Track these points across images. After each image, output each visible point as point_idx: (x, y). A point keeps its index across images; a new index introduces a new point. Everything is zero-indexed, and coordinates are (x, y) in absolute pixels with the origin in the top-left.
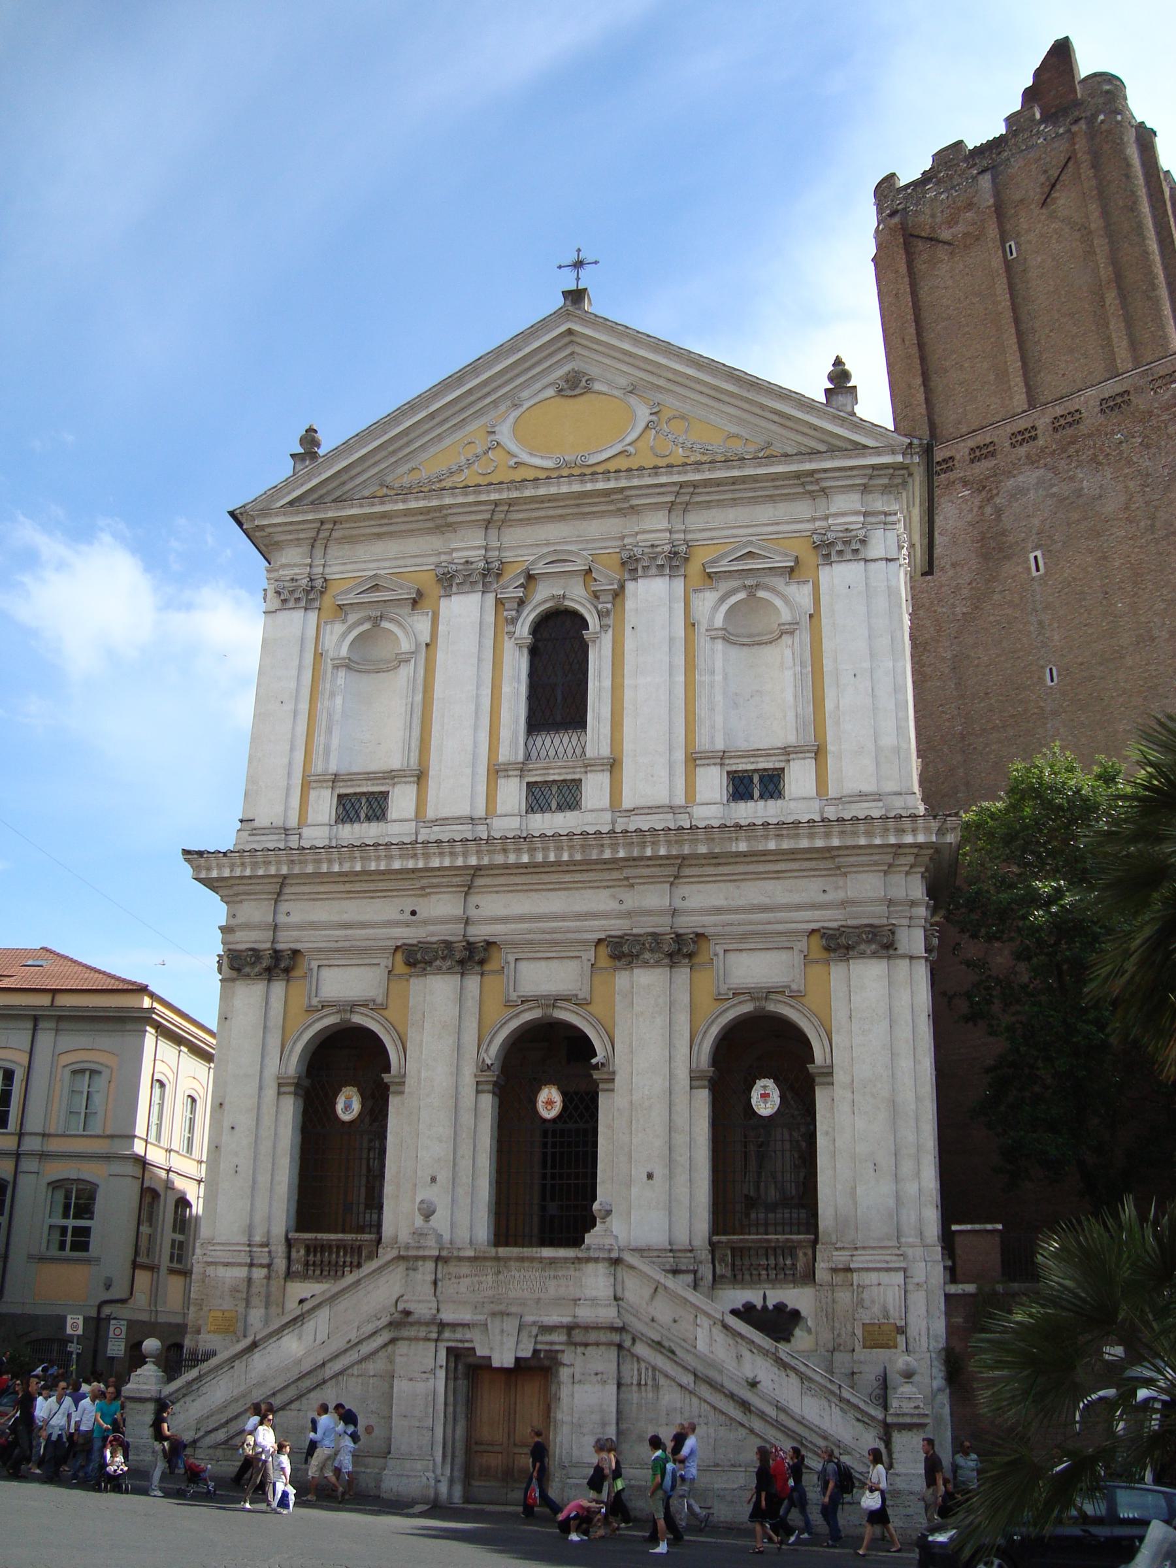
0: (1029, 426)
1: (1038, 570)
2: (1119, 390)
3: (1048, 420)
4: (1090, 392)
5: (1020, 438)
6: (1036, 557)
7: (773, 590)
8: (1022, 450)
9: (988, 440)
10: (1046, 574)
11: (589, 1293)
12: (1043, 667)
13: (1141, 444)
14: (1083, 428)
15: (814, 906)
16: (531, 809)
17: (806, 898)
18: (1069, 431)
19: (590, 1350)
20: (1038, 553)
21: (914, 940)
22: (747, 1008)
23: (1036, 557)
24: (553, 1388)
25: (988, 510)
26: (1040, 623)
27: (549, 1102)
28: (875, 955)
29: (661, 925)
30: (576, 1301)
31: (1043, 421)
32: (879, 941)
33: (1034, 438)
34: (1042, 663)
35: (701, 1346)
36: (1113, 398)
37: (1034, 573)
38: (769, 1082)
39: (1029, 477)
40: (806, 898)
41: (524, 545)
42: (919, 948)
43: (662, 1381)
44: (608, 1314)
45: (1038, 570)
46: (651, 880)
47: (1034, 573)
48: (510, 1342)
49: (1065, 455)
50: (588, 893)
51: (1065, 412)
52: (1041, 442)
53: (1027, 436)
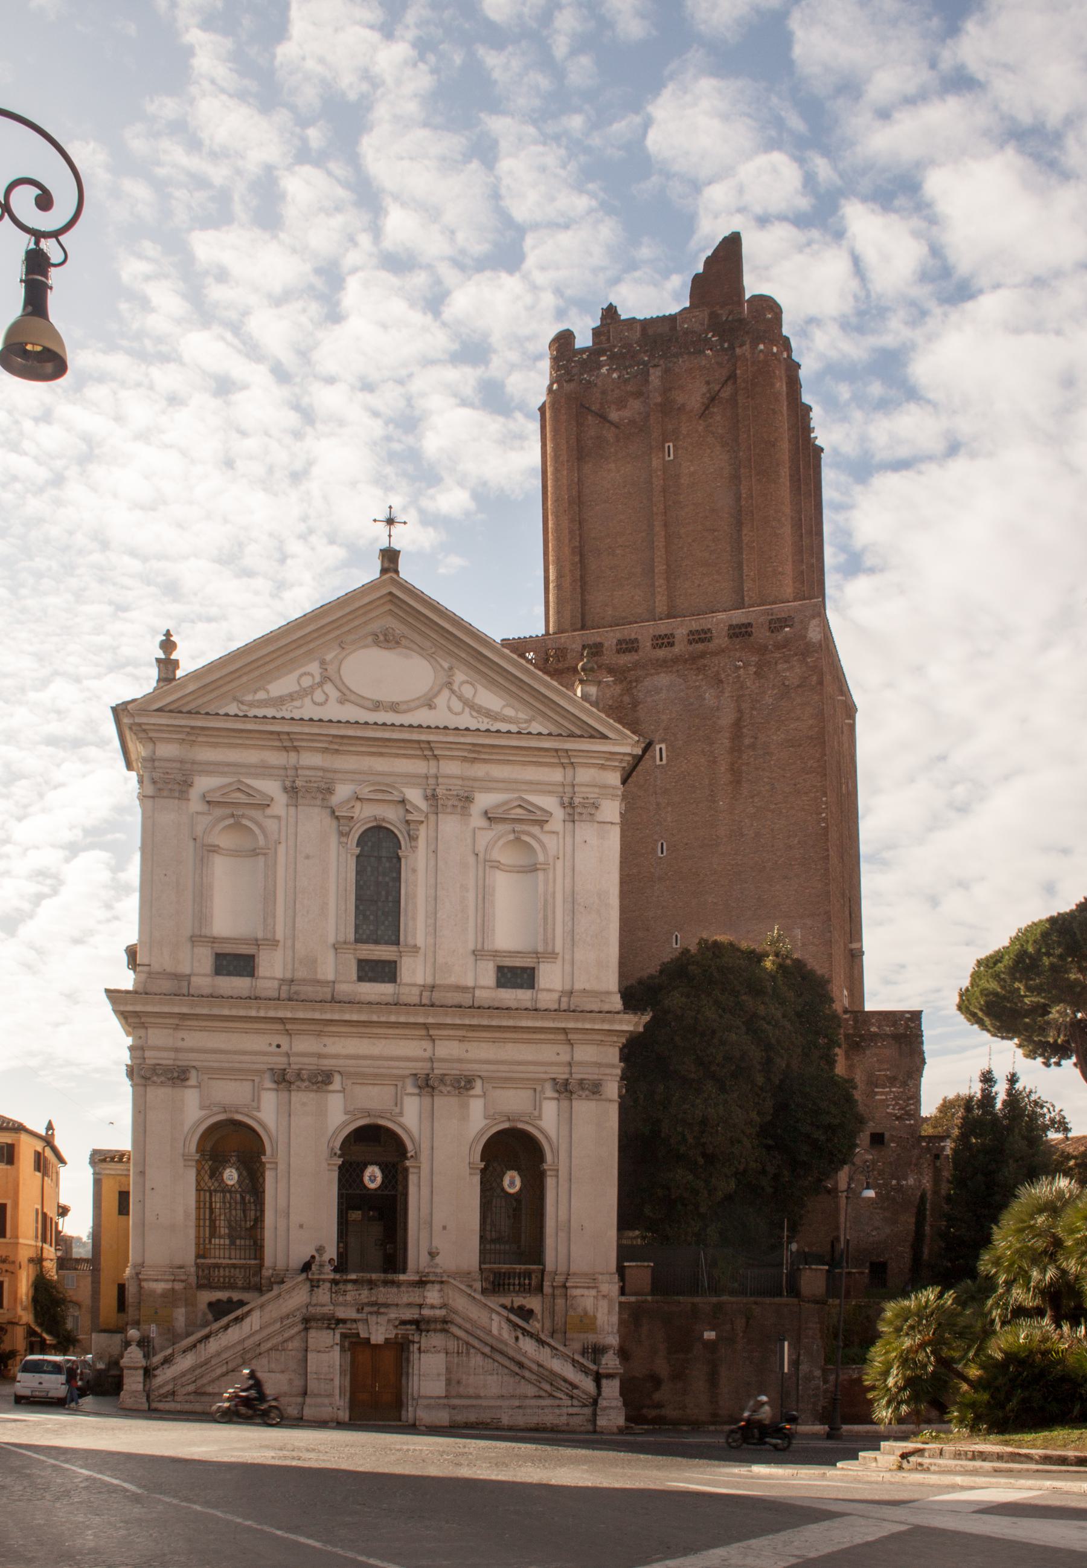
0: (668, 632)
1: (661, 760)
2: (746, 621)
3: (685, 632)
4: (722, 616)
5: (660, 641)
6: (661, 749)
7: (534, 837)
8: (661, 653)
9: (633, 636)
10: (667, 764)
11: (429, 1301)
12: (657, 841)
13: (755, 673)
14: (712, 646)
15: (552, 1064)
16: (360, 979)
17: (548, 1056)
18: (700, 646)
19: (432, 1334)
20: (663, 746)
21: (612, 1089)
22: (506, 1125)
23: (661, 749)
24: (404, 1356)
25: (626, 699)
26: (658, 804)
27: (373, 1177)
28: (587, 1098)
29: (454, 1070)
30: (420, 1306)
31: (681, 632)
32: (594, 1089)
33: (671, 644)
34: (656, 837)
35: (495, 1331)
36: (740, 626)
37: (658, 762)
38: (515, 1173)
39: (663, 679)
40: (548, 1056)
41: (352, 776)
42: (615, 1096)
43: (472, 1351)
44: (440, 1313)
45: (661, 760)
46: (449, 1038)
47: (658, 762)
48: (382, 1329)
49: (694, 666)
50: (402, 1043)
51: (699, 628)
52: (676, 649)
53: (664, 641)
